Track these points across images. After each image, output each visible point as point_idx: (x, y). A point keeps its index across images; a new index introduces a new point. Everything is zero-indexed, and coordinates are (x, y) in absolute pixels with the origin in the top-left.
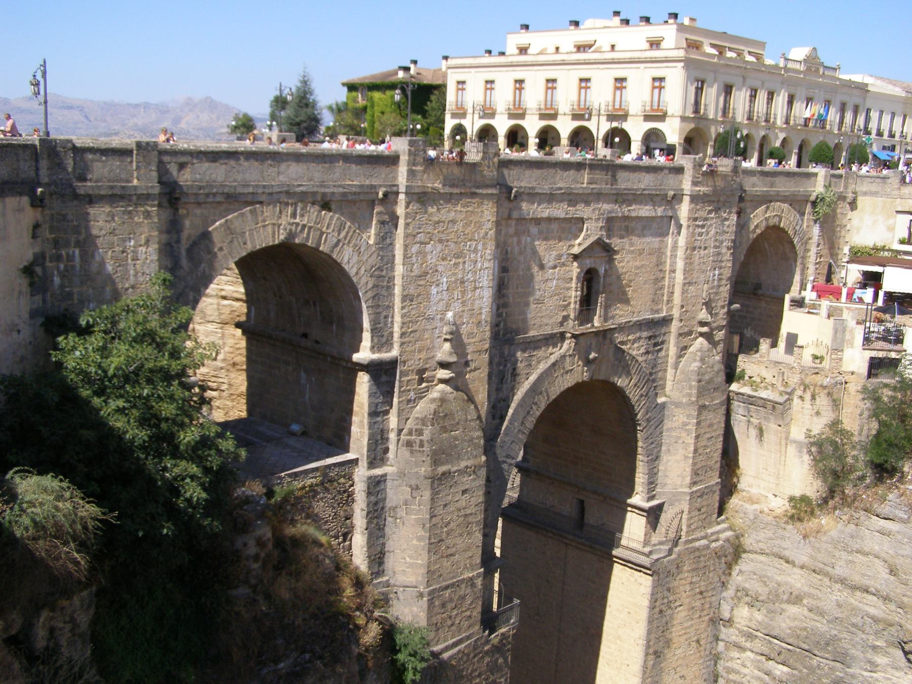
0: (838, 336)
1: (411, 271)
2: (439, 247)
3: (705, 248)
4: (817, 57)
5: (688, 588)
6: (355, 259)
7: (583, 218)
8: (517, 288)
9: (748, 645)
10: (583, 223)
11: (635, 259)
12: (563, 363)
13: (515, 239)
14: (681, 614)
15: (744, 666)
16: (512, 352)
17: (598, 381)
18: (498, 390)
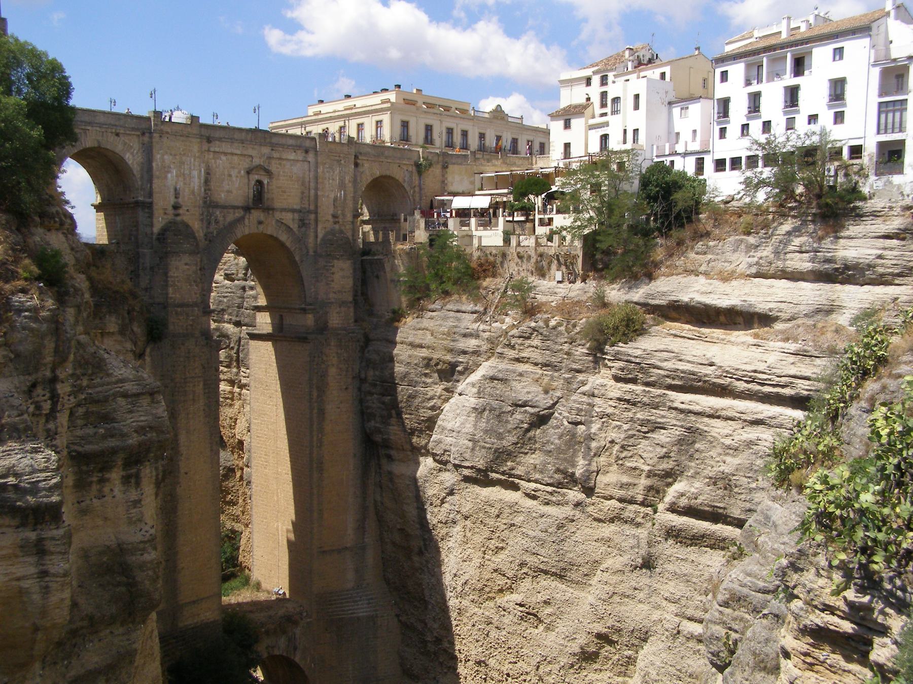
1: (158, 165)
2: (171, 157)
6: (131, 157)
9: (374, 391)
13: (213, 161)
14: (333, 371)
15: (373, 403)
18: (208, 227)
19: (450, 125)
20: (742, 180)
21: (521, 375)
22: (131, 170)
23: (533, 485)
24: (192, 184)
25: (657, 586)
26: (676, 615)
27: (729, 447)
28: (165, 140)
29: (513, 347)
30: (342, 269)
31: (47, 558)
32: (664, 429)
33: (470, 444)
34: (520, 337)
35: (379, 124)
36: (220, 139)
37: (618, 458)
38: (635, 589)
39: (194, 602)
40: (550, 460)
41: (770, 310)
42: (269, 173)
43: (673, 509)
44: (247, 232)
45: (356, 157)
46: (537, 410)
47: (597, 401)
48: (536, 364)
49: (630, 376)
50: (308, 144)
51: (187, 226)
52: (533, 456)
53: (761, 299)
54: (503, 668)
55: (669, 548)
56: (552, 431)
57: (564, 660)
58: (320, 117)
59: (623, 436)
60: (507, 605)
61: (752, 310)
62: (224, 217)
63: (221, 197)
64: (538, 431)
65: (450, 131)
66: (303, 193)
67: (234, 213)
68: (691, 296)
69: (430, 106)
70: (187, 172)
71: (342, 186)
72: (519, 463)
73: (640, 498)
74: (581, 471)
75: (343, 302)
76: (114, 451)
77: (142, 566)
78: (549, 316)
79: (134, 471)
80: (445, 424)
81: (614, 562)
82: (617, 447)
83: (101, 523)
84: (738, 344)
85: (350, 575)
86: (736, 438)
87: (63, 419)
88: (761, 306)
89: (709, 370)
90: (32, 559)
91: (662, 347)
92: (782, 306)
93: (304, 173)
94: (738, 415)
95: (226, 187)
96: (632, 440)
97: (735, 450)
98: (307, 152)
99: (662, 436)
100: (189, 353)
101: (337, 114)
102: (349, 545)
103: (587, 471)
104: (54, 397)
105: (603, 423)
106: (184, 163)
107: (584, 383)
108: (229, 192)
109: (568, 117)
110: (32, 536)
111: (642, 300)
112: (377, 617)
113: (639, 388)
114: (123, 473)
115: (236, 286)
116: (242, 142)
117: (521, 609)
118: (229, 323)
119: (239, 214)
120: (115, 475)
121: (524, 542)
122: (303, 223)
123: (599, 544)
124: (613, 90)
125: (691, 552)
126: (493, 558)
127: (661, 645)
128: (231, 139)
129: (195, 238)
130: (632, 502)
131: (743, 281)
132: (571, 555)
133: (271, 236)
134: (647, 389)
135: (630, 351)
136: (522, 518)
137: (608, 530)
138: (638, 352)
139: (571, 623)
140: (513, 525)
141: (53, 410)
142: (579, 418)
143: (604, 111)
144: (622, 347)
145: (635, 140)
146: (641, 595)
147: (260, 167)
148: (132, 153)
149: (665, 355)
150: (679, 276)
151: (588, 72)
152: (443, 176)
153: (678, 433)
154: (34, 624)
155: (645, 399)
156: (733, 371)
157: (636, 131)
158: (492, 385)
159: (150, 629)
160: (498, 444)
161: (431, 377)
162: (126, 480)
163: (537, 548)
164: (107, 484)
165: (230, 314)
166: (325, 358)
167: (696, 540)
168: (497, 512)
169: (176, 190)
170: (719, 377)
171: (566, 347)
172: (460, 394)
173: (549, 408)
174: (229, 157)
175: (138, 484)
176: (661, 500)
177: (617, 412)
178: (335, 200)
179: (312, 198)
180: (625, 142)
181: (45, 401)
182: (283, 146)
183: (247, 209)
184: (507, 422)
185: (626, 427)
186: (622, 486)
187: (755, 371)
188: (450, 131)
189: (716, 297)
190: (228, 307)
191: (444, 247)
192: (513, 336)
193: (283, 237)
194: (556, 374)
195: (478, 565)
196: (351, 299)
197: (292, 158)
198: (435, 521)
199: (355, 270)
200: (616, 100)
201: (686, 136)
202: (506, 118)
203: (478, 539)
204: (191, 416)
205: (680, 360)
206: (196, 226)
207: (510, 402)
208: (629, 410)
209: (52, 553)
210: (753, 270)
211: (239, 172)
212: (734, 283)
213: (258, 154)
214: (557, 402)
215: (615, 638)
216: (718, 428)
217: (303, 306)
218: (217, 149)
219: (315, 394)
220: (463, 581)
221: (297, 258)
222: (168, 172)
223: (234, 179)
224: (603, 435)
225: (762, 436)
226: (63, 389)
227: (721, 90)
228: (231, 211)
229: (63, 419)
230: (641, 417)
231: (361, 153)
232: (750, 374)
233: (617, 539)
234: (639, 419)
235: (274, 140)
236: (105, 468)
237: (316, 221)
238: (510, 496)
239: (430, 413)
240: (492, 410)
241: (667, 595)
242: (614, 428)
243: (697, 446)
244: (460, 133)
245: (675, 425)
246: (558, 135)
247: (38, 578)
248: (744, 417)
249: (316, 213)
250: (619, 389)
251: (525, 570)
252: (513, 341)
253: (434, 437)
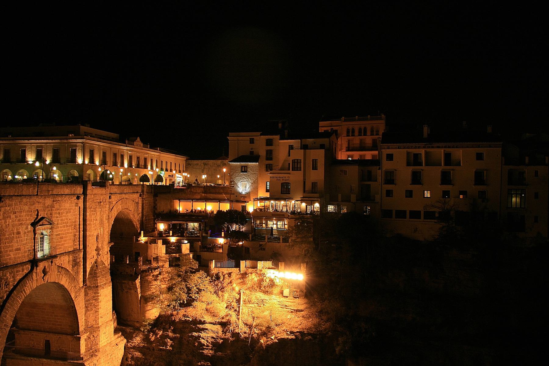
0: (155, 251)
3: (96, 220)
7: (37, 210)
8: (6, 244)
10: (38, 212)
11: (64, 227)
12: (32, 277)
16: (5, 274)
67: (23, 270)
95: (15, 245)
98: (78, 198)
128: (20, 196)
221: (73, 296)
228: (20, 269)
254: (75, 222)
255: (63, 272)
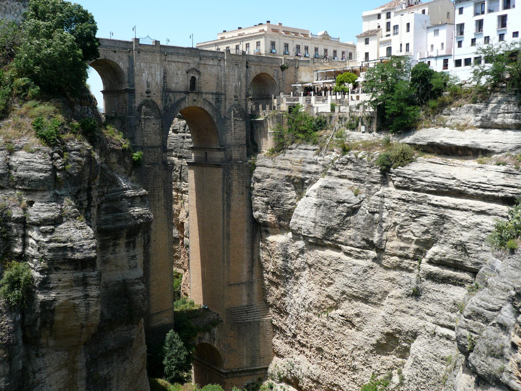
4: (328, 35)
5: (236, 174)
14: (235, 183)
17: (197, 107)
18: (165, 103)
19: (299, 44)
20: (472, 71)
21: (341, 185)
22: (123, 72)
23: (349, 248)
24: (156, 79)
25: (422, 306)
26: (433, 323)
27: (464, 226)
28: (141, 54)
29: (337, 170)
30: (240, 126)
31: (89, 287)
32: (426, 216)
33: (313, 224)
34: (341, 164)
35: (258, 44)
36: (171, 54)
37: (398, 233)
38: (409, 308)
39: (159, 313)
40: (359, 233)
41: (489, 147)
42: (199, 72)
43: (431, 262)
44: (187, 106)
45: (247, 63)
46: (351, 205)
47: (386, 200)
48: (350, 179)
49: (405, 186)
50: (220, 55)
51: (154, 103)
52: (349, 231)
53: (483, 141)
54: (332, 352)
55: (428, 284)
56: (359, 217)
57: (367, 348)
58: (225, 40)
59: (401, 220)
60: (334, 316)
61: (477, 147)
62: (174, 97)
63: (173, 86)
64: (352, 217)
65: (298, 47)
66: (218, 83)
68: (441, 139)
69: (287, 32)
70: (153, 72)
71: (239, 79)
72: (341, 235)
73: (411, 255)
74: (377, 240)
75: (240, 145)
76: (122, 228)
77: (137, 293)
78: (358, 151)
79: (132, 239)
80: (299, 213)
81: (396, 292)
82: (397, 227)
83: (114, 268)
84: (469, 167)
85: (245, 298)
86: (469, 221)
87: (94, 211)
88: (483, 145)
89: (452, 182)
90: (80, 288)
91: (424, 169)
92: (496, 144)
93: (218, 73)
94: (470, 208)
95: (176, 81)
96: (407, 222)
97: (468, 228)
99: (424, 220)
100: (156, 173)
101: (234, 38)
102: (244, 281)
103: (380, 239)
104: (90, 199)
105: (390, 212)
106: (152, 68)
107: (378, 190)
108: (177, 83)
109: (367, 38)
110: (80, 275)
111: (412, 142)
112: (260, 322)
113: (411, 193)
114: (127, 241)
115: (179, 136)
116: (184, 55)
117: (342, 318)
118: (176, 156)
119: (182, 96)
120: (122, 242)
121: (344, 280)
122: (218, 101)
123: (387, 282)
124: (394, 20)
125: (442, 287)
126: (326, 289)
127: (425, 341)
129: (159, 109)
130: (407, 257)
131: (472, 130)
132: (371, 288)
133: (200, 108)
134: (416, 193)
135: (405, 171)
136: (342, 266)
137: (392, 274)
138: (410, 172)
139: (371, 327)
140: (337, 270)
141: (89, 205)
142: (375, 210)
143: (388, 33)
144: (400, 169)
145: (407, 50)
146: (412, 312)
147: (193, 69)
148: (123, 62)
149: (426, 173)
150: (434, 128)
151: (379, 11)
152: (296, 73)
153: (434, 218)
154: (81, 324)
155: (414, 199)
156: (467, 182)
157: (408, 45)
158: (325, 191)
159: (140, 327)
160: (329, 224)
161: (290, 187)
162: (128, 245)
163: (351, 284)
164: (117, 247)
165: (176, 152)
166: (231, 176)
167: (446, 280)
168: (328, 263)
169: (147, 82)
170: (458, 186)
171: (368, 169)
172: (307, 196)
173: (358, 204)
174: (177, 63)
175: (134, 247)
176: (424, 257)
177: (398, 206)
178: (236, 87)
179: (223, 86)
180: (401, 51)
181: (84, 201)
182: (206, 57)
183: (187, 93)
184: (334, 212)
185: (403, 215)
186: (401, 248)
187: (480, 183)
188: (298, 47)
189: (456, 140)
190: (175, 148)
191: (297, 113)
192: (337, 163)
193: (207, 109)
194: (362, 185)
195: (318, 293)
196: (245, 143)
197: (212, 64)
198: (293, 268)
199: (247, 126)
200: (396, 27)
201: (437, 46)
202: (330, 39)
203: (317, 278)
204: (157, 209)
205: (435, 176)
206: (159, 102)
207: (336, 201)
208: (405, 205)
209: (91, 285)
210: (478, 124)
211: (182, 72)
212: (467, 131)
213: (193, 62)
214: (362, 201)
215: (397, 336)
216: (457, 215)
217: (218, 147)
218: (170, 59)
219: (225, 196)
220: (309, 302)
221: (215, 120)
222: (143, 72)
223: (180, 76)
224: (390, 219)
225: (484, 220)
226: (95, 193)
227: (459, 19)
228: (178, 94)
229: (94, 211)
230: (412, 209)
231: (250, 61)
232: (477, 184)
233: (398, 279)
234: (410, 210)
235: (202, 54)
236: (117, 237)
237: (225, 99)
238: (335, 254)
239: (290, 207)
240: (325, 205)
241: (428, 311)
242: (396, 215)
243: (445, 225)
244: (304, 48)
245: (432, 214)
246: (361, 48)
247: (83, 298)
248: (473, 209)
249: (225, 95)
250: (399, 193)
251: (345, 296)
252: (337, 166)
253: (292, 220)
254: (218, 75)
255: (207, 103)
